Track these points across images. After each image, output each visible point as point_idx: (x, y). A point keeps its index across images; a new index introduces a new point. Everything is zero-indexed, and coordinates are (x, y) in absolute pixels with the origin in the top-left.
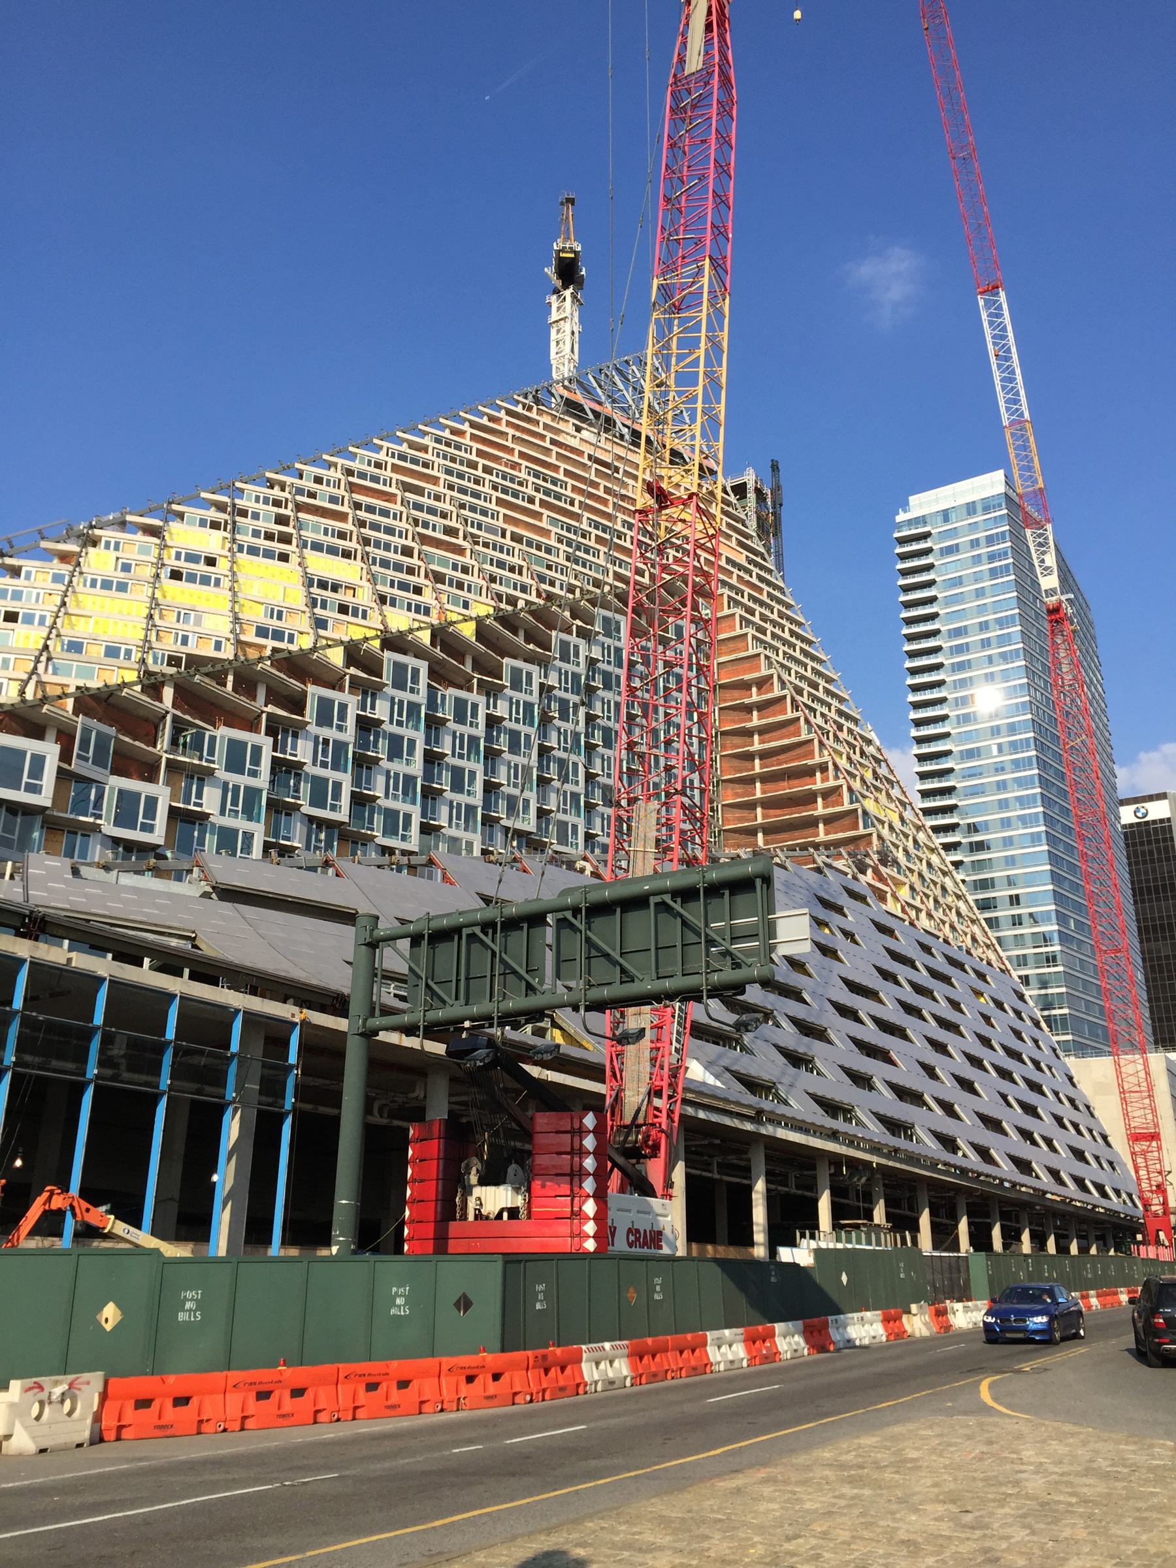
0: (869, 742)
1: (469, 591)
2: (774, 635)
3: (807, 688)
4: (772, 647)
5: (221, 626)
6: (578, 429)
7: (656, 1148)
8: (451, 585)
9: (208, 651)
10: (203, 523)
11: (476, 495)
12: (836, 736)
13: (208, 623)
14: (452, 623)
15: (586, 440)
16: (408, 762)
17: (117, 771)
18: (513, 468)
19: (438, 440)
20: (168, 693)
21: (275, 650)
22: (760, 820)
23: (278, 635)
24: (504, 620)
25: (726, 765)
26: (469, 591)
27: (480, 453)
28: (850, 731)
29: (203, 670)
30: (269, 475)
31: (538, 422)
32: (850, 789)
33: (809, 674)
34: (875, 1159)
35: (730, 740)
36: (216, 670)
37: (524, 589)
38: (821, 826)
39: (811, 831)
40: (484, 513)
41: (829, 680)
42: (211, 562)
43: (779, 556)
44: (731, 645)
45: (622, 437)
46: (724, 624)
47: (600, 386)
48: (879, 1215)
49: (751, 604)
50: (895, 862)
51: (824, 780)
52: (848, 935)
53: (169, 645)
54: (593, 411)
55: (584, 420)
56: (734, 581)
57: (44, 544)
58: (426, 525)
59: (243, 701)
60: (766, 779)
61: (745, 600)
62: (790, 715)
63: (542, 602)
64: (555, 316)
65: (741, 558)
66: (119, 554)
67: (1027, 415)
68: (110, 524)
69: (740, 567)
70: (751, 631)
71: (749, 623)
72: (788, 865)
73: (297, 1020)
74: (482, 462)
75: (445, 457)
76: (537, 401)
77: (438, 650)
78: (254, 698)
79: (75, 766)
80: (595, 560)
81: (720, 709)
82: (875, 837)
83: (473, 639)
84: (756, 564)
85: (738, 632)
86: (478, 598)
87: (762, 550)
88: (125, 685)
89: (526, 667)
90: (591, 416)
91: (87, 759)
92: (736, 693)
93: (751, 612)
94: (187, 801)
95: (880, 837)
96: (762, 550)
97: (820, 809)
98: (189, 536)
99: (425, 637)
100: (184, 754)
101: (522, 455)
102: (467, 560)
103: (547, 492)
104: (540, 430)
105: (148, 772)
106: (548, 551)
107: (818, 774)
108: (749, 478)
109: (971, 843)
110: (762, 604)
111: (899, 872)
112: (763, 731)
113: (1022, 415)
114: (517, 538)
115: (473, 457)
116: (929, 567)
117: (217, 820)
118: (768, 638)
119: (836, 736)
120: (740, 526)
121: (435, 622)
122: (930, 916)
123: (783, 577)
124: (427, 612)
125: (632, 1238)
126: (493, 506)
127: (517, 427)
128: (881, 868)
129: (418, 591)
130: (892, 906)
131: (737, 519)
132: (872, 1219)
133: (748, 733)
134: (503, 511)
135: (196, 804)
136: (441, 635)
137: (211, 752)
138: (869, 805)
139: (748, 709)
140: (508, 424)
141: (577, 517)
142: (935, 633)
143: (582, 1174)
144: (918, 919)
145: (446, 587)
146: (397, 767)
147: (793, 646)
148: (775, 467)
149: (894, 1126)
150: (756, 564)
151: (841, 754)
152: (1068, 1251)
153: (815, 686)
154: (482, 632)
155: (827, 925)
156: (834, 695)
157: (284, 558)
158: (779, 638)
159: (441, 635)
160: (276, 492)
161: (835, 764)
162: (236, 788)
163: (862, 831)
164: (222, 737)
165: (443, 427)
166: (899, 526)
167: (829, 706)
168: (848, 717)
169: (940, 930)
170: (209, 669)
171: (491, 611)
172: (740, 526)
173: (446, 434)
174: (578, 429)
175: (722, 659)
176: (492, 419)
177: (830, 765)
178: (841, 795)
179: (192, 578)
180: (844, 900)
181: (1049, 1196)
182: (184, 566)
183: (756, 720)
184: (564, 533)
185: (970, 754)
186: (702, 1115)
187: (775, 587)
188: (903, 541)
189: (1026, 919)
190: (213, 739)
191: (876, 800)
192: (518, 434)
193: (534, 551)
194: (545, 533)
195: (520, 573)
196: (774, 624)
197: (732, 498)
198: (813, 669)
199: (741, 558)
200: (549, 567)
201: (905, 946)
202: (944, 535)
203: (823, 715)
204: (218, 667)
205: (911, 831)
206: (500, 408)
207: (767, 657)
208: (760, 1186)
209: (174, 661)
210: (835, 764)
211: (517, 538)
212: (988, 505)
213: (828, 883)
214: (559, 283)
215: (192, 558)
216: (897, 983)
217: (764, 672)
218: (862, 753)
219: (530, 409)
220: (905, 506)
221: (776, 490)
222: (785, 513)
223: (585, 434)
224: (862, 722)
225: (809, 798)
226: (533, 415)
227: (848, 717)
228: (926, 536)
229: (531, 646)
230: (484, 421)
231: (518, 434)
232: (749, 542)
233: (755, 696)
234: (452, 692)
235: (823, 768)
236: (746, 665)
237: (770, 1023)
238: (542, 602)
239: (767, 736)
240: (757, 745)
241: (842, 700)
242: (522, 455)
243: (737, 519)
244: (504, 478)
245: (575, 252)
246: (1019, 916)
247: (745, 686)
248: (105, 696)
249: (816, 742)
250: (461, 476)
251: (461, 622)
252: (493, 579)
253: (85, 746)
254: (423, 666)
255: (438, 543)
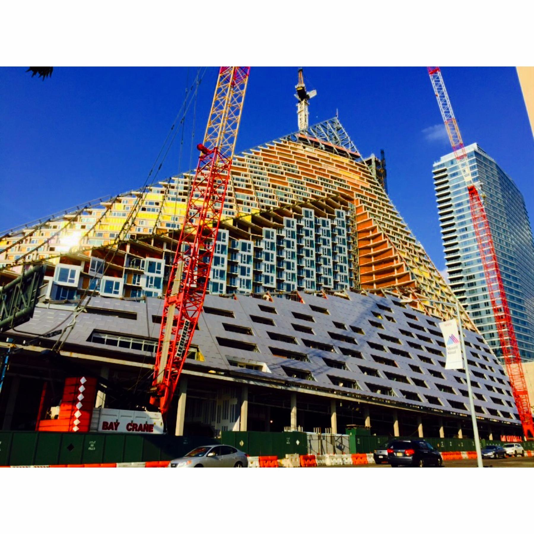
0: (419, 248)
1: (252, 205)
2: (379, 212)
3: (391, 230)
4: (377, 216)
5: (152, 224)
6: (304, 147)
7: (163, 392)
8: (245, 204)
9: (148, 233)
10: (158, 192)
11: (261, 173)
12: (402, 247)
13: (147, 224)
14: (241, 217)
15: (310, 150)
16: (223, 266)
17: (106, 274)
18: (277, 163)
19: (249, 157)
20: (128, 247)
21: (170, 230)
22: (374, 279)
23: (174, 226)
24: (262, 214)
25: (362, 260)
26: (252, 205)
27: (264, 159)
28: (410, 244)
29: (140, 239)
30: (184, 174)
31: (288, 147)
32: (406, 265)
33: (394, 225)
34: (359, 401)
35: (362, 252)
36: (147, 239)
37: (274, 203)
38: (397, 280)
39: (393, 282)
40: (263, 179)
41: (403, 227)
42: (157, 204)
43: (386, 184)
44: (362, 217)
45: (322, 148)
46: (358, 210)
47: (315, 132)
48: (367, 423)
49: (371, 202)
50: (424, 291)
51: (397, 262)
52: (389, 318)
53: (134, 231)
54: (310, 141)
55: (307, 144)
56: (364, 194)
57: (102, 203)
58: (239, 185)
59: (156, 248)
60: (376, 264)
61: (368, 201)
62: (383, 240)
63: (279, 207)
64: (299, 110)
65: (368, 185)
66: (125, 204)
67: (453, 116)
68: (126, 195)
69: (367, 189)
70: (368, 211)
71: (368, 209)
72: (367, 293)
73: (9, 347)
74: (264, 162)
75: (251, 162)
76: (289, 139)
77: (236, 228)
78: (162, 247)
79: (90, 273)
80: (305, 191)
81: (359, 240)
82: (416, 283)
83: (250, 222)
84: (374, 188)
85: (364, 212)
86: (255, 208)
87: (377, 182)
88: (109, 245)
89: (271, 230)
90: (310, 142)
91: (94, 271)
92: (364, 234)
93: (370, 205)
94: (134, 283)
95: (418, 283)
96: (377, 182)
97: (396, 274)
98: (154, 195)
99: (230, 223)
100: (132, 267)
101: (281, 158)
102: (253, 196)
103: (289, 170)
104: (289, 149)
105: (119, 274)
106: (286, 190)
107: (395, 261)
108: (373, 157)
109: (468, 284)
110: (375, 201)
111: (427, 295)
112: (375, 247)
113: (451, 117)
114: (274, 187)
115: (262, 161)
116: (447, 182)
117: (145, 289)
118: (377, 213)
119: (402, 247)
120: (369, 175)
121: (234, 217)
122: (438, 310)
123: (387, 192)
124: (233, 214)
125: (130, 427)
126: (267, 177)
127: (280, 149)
128: (416, 294)
129: (231, 207)
130: (420, 308)
131: (367, 173)
132: (364, 424)
133: (369, 248)
134: (269, 178)
135: (138, 284)
136: (236, 221)
137: (143, 266)
138: (415, 271)
139: (368, 239)
140: (277, 148)
141: (300, 177)
142: (450, 206)
143: (77, 401)
144: (433, 312)
145: (243, 205)
146: (219, 268)
147: (388, 215)
148: (382, 152)
149: (386, 390)
150: (374, 188)
151: (404, 253)
152: (488, 438)
153: (396, 229)
154: (254, 219)
155: (380, 315)
156: (404, 232)
157: (184, 200)
158: (382, 213)
159: (236, 221)
160: (187, 180)
161: (400, 257)
162: (152, 278)
163: (411, 281)
164: (147, 261)
165: (251, 153)
166: (434, 168)
167: (402, 236)
168: (410, 239)
169: (442, 316)
170: (142, 238)
171: (259, 211)
172: (369, 175)
173: (253, 154)
174: (304, 147)
175: (358, 223)
176: (271, 147)
177: (399, 257)
178: (403, 268)
179: (149, 210)
180: (393, 307)
181: (461, 415)
182: (147, 206)
183: (372, 243)
184: (294, 183)
185: (466, 250)
186: (252, 383)
187: (382, 195)
188: (436, 173)
189: (492, 311)
190: (144, 262)
191: (418, 269)
192: (280, 151)
193: (281, 190)
194: (286, 184)
195: (273, 198)
196: (380, 208)
197: (366, 165)
198: (396, 223)
199: (368, 185)
200: (286, 195)
201: (419, 322)
202: (452, 169)
203: (398, 239)
204: (146, 237)
205: (434, 280)
206: (273, 144)
207: (374, 220)
208: (294, 411)
209: (132, 237)
210: (400, 257)
211: (274, 187)
212: (469, 155)
213: (386, 300)
214: (300, 99)
215: (151, 203)
216: (412, 336)
217: (374, 225)
218: (415, 253)
219: (286, 142)
220: (438, 159)
221: (383, 159)
222: (386, 168)
223: (307, 149)
224: (416, 241)
225: (392, 270)
226: (287, 144)
227: (410, 239)
228: (445, 170)
229: (275, 223)
230: (268, 149)
231: (280, 151)
232: (372, 180)
233: (371, 234)
234: (241, 241)
235: (396, 258)
236: (367, 223)
237: (332, 350)
238: (279, 207)
239: (375, 249)
240: (372, 252)
241: (408, 233)
242: (281, 158)
243: (367, 173)
244: (273, 167)
245: (303, 88)
246: (489, 310)
247: (367, 231)
248: (103, 249)
249: (393, 249)
250: (256, 168)
251: (244, 216)
252: (262, 201)
253: (93, 266)
254: (227, 232)
255: (243, 191)
